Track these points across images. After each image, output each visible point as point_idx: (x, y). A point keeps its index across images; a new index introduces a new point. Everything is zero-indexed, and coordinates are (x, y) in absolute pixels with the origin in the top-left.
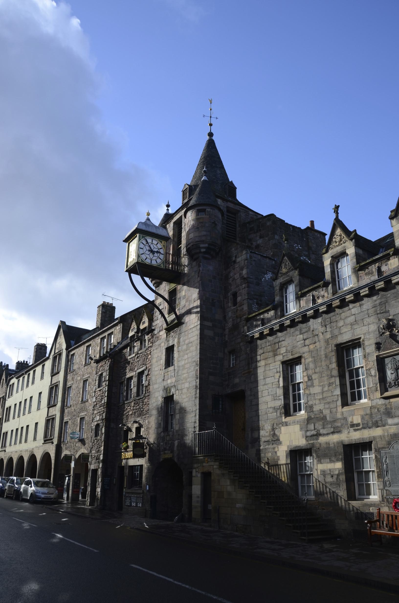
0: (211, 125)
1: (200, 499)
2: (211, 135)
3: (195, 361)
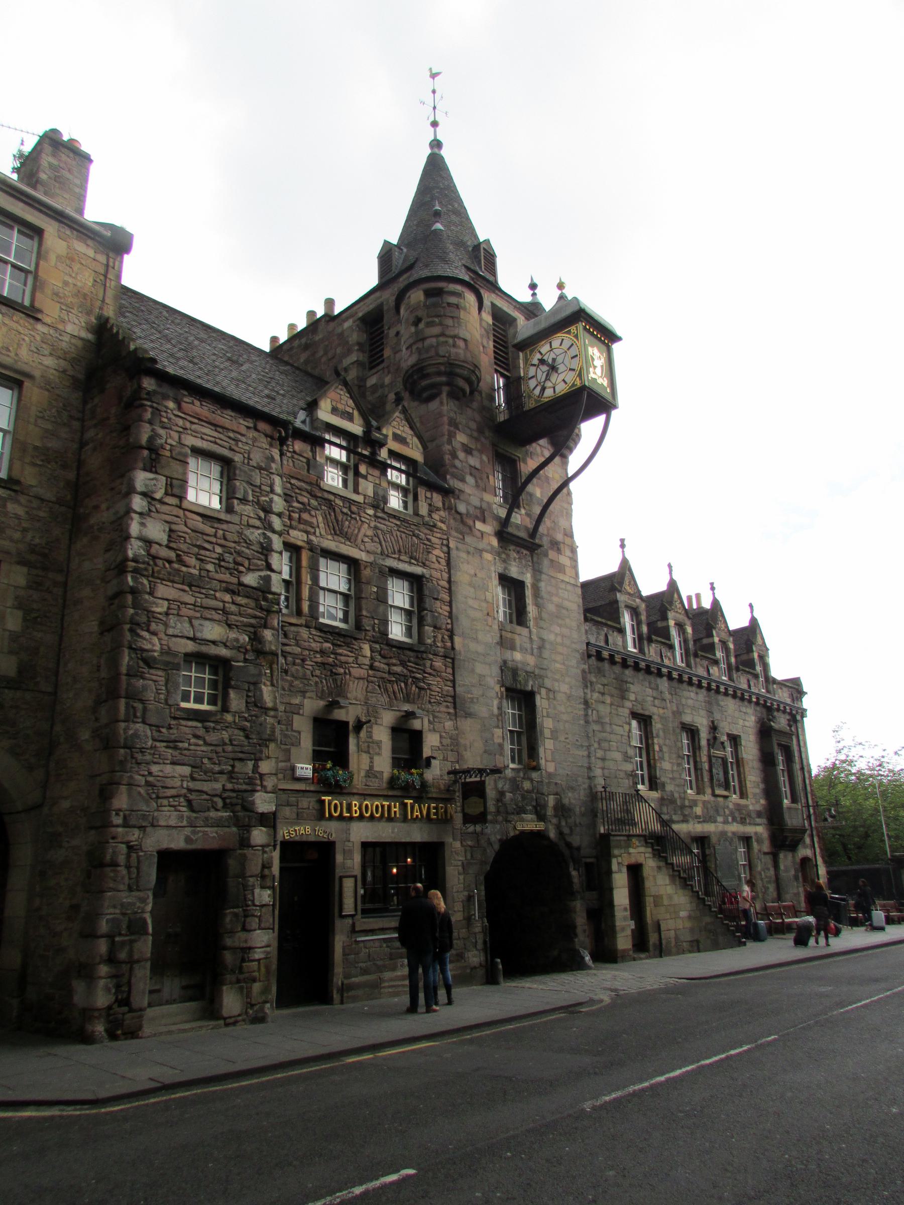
0: (435, 124)
1: (628, 913)
2: (436, 144)
3: (578, 651)
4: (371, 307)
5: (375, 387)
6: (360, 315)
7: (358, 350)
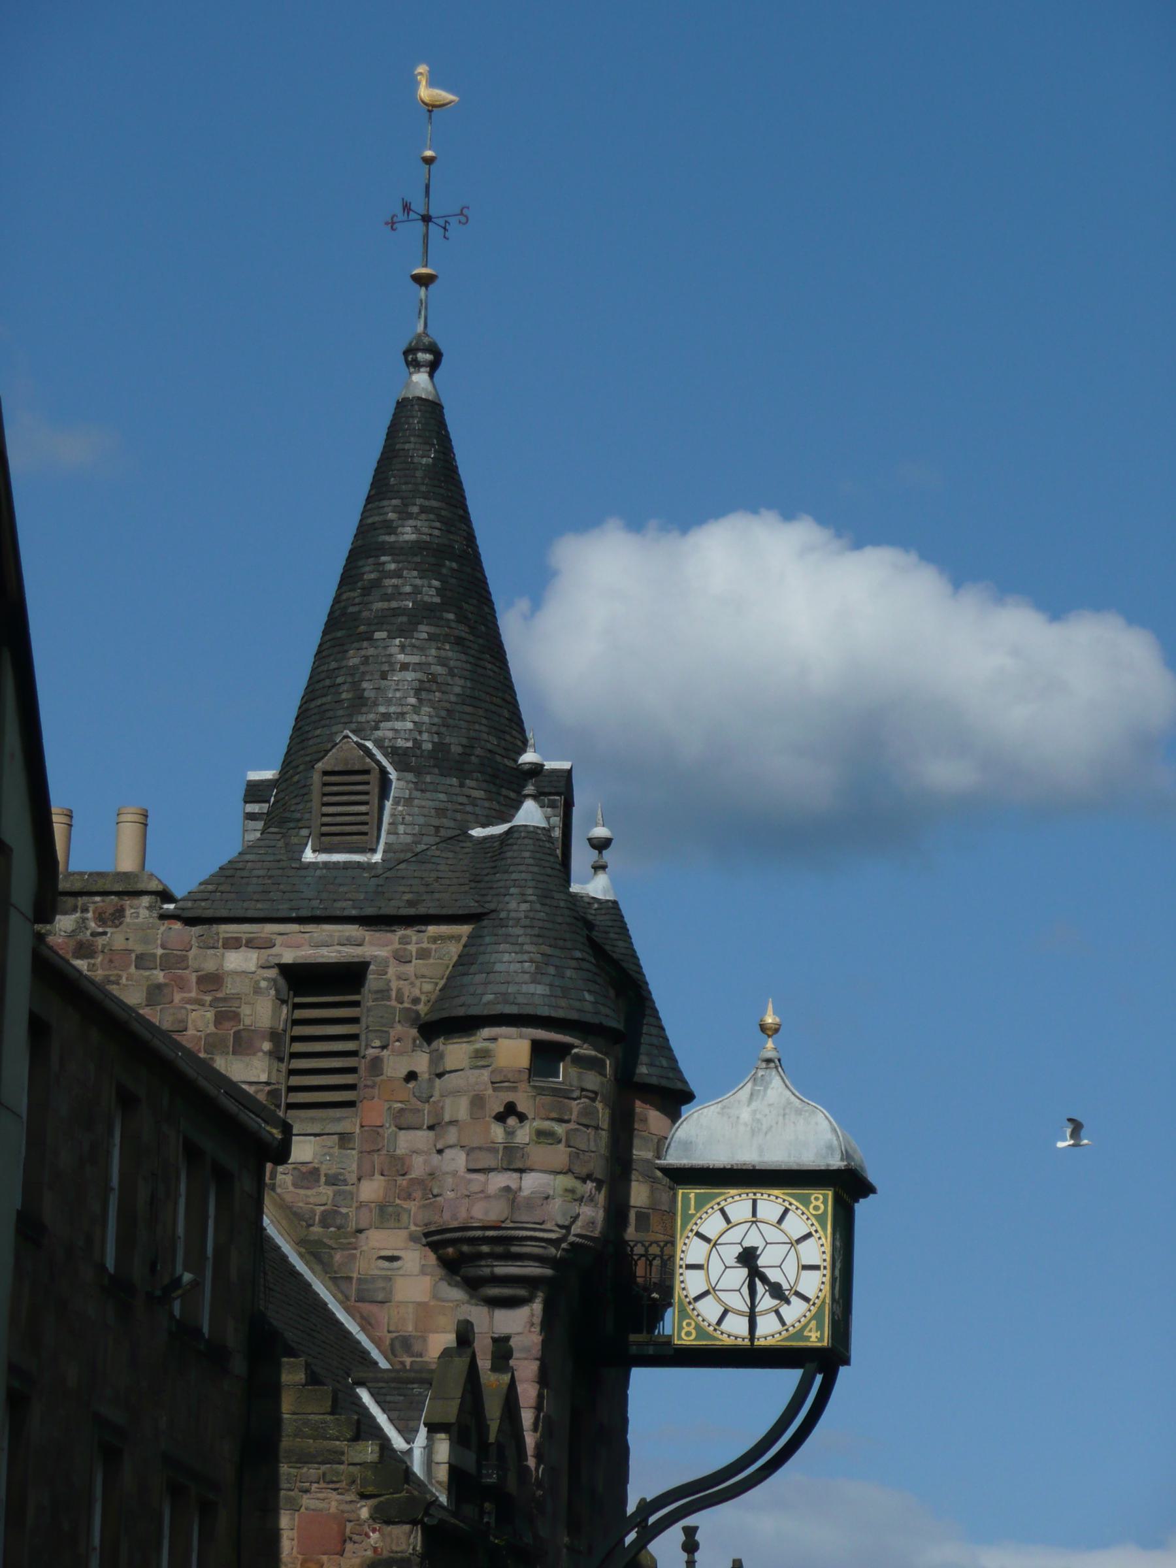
4: (329, 955)
5: (309, 1176)
6: (288, 957)
7: (270, 1053)
